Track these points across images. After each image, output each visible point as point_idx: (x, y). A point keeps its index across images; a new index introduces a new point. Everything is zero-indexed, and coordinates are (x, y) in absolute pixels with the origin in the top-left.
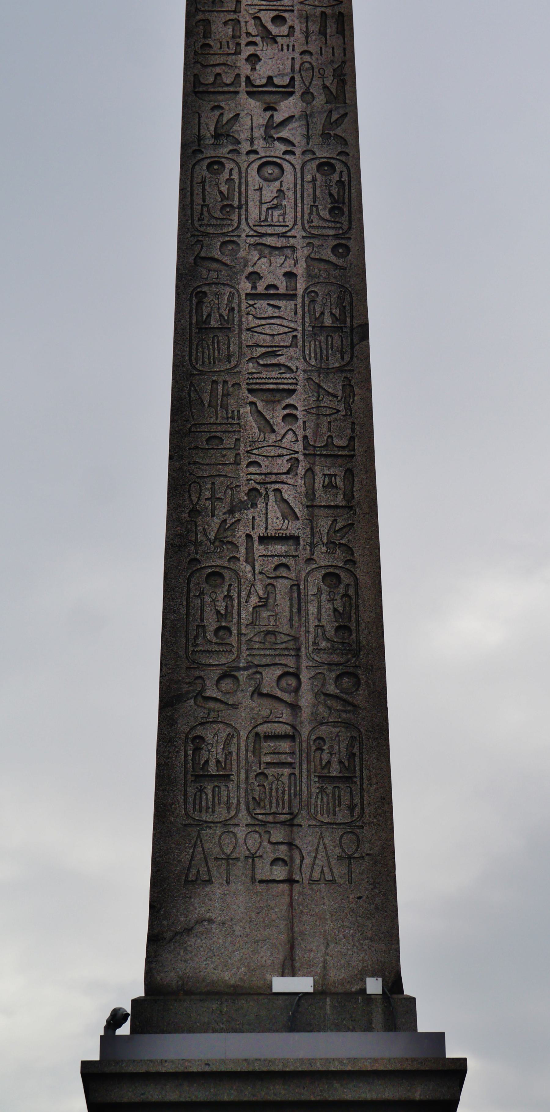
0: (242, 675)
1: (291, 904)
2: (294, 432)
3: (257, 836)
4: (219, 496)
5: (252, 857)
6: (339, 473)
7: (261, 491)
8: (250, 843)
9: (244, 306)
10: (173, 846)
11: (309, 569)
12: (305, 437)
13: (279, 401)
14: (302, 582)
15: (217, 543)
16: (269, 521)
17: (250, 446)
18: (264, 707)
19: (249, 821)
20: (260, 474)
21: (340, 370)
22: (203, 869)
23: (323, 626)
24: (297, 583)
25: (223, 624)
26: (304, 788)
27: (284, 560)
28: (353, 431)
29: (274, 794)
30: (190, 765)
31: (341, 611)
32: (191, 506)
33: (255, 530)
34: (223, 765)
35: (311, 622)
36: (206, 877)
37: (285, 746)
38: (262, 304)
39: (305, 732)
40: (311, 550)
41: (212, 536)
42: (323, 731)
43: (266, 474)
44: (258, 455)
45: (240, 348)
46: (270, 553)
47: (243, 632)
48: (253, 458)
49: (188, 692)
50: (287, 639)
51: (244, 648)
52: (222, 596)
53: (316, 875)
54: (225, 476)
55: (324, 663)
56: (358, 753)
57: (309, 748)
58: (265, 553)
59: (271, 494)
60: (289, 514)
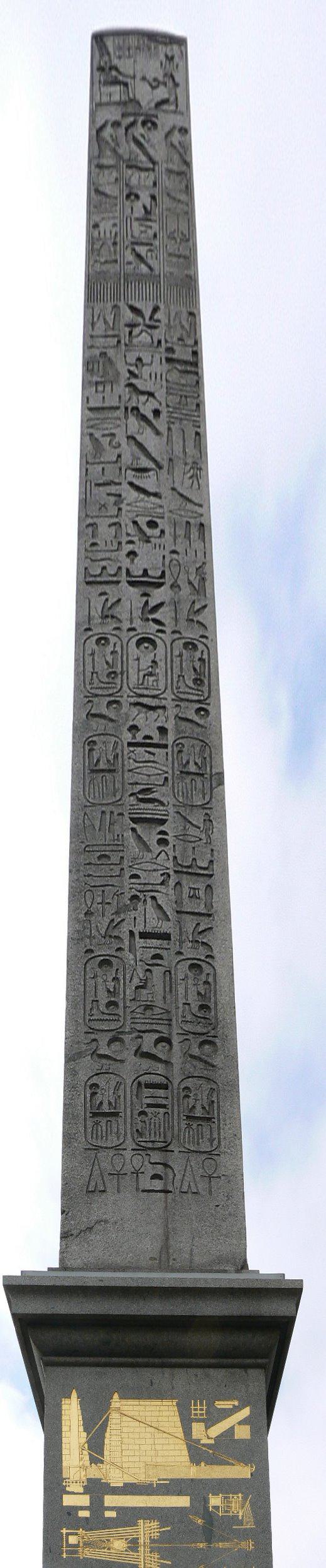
0: (127, 1038)
2: (166, 853)
3: (140, 1157)
4: (108, 901)
5: (137, 1173)
6: (201, 888)
7: (141, 897)
8: (135, 1162)
9: (125, 753)
10: (77, 1164)
11: (178, 959)
12: (175, 858)
14: (173, 969)
15: (107, 938)
16: (147, 920)
17: (132, 862)
18: (146, 1064)
20: (139, 884)
21: (203, 807)
22: (100, 1182)
23: (189, 1004)
24: (168, 969)
25: (112, 999)
26: (176, 1123)
27: (158, 951)
28: (212, 855)
29: (152, 1126)
30: (88, 1105)
31: (203, 994)
32: (87, 909)
33: (136, 927)
34: (114, 1104)
35: (180, 1000)
36: (102, 1188)
38: (140, 750)
39: (176, 1083)
40: (179, 945)
41: (103, 932)
42: (189, 1083)
43: (145, 884)
44: (139, 869)
45: (123, 784)
46: (148, 946)
47: (127, 1005)
48: (135, 872)
49: (86, 1050)
52: (112, 978)
53: (185, 1189)
54: (112, 885)
55: (190, 1032)
56: (216, 1101)
57: (178, 1093)
58: (144, 945)
59: (149, 900)
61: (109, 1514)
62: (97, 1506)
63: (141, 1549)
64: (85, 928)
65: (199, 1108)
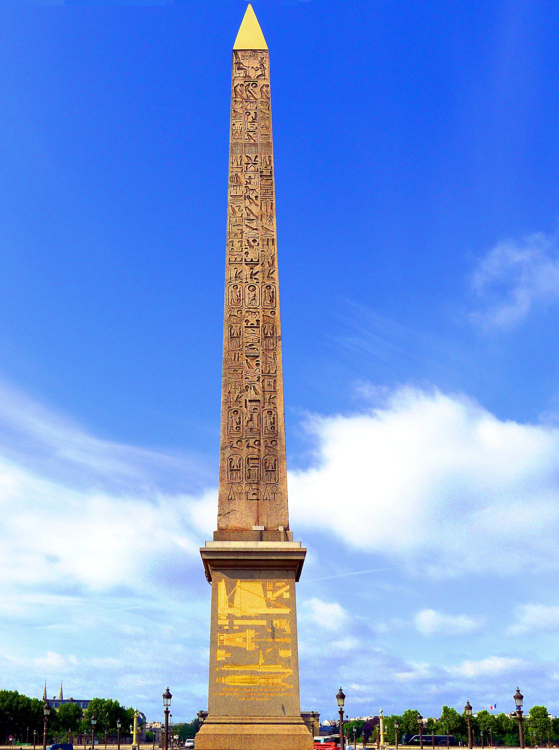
1: (258, 506)
12: (262, 370)
13: (255, 359)
19: (246, 482)
27: (256, 407)
37: (256, 461)
42: (267, 457)
48: (247, 376)
50: (256, 430)
59: (252, 388)
61: (235, 628)
62: (231, 624)
63: (248, 641)
64: (228, 398)
65: (270, 467)
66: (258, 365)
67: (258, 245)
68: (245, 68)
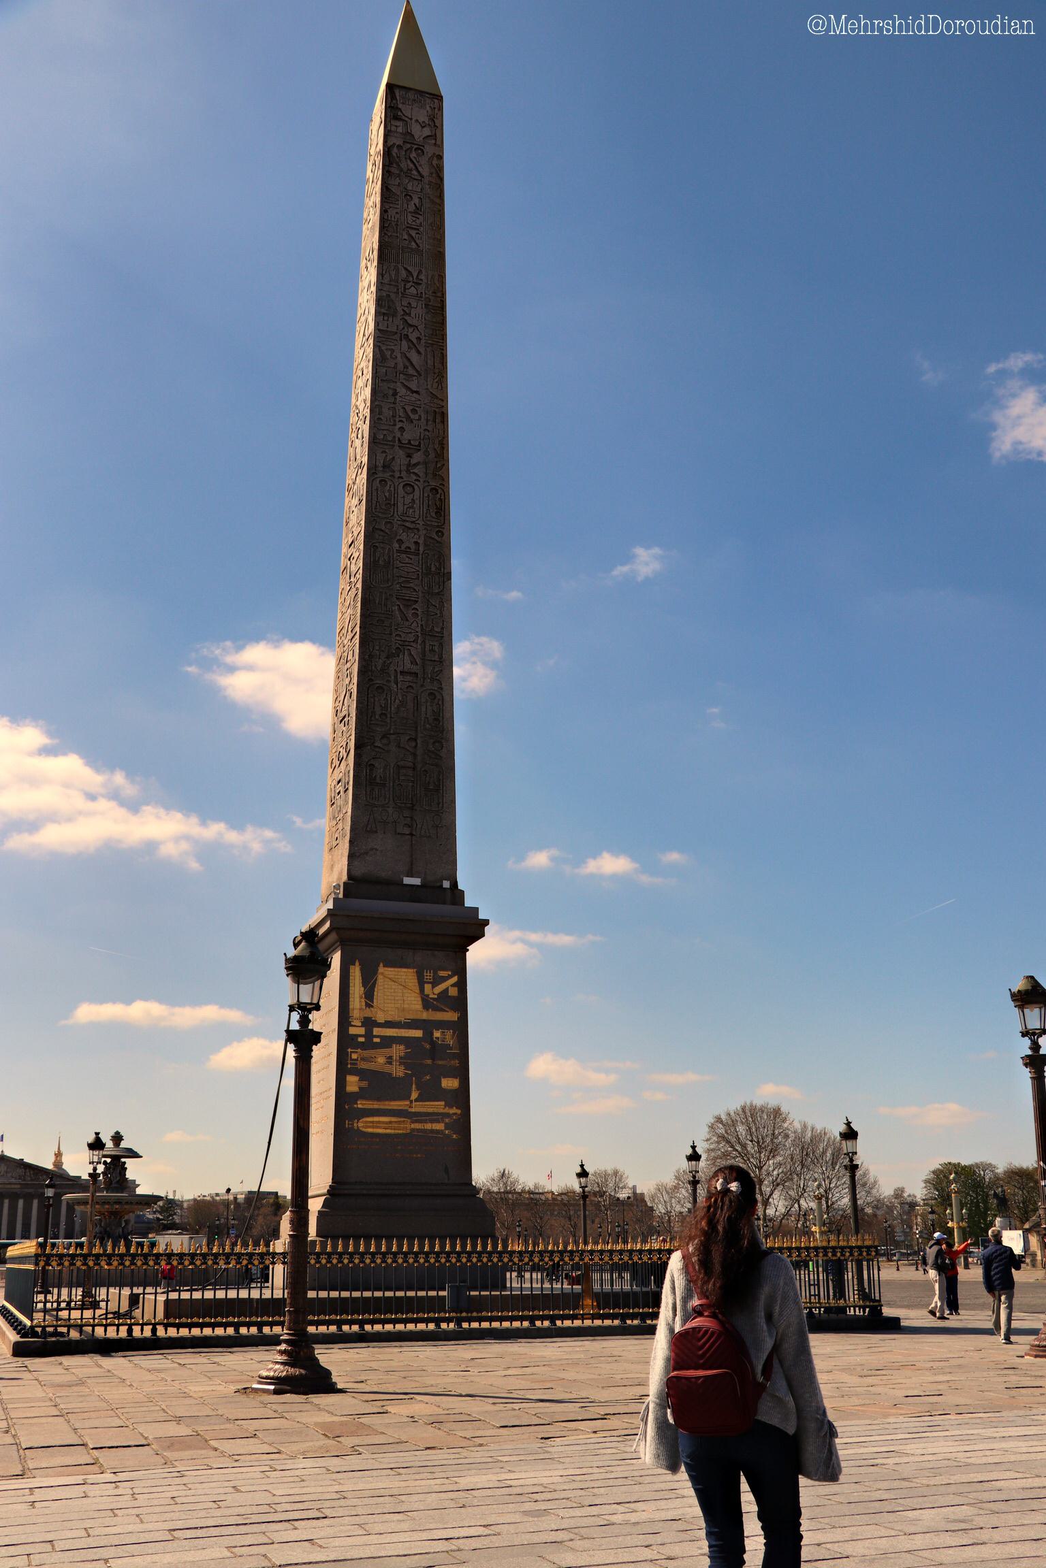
9: (395, 555)
12: (422, 625)
43: (404, 641)
45: (393, 577)
51: (393, 724)
60: (414, 662)
66: (416, 615)
67: (420, 419)
68: (406, 119)
